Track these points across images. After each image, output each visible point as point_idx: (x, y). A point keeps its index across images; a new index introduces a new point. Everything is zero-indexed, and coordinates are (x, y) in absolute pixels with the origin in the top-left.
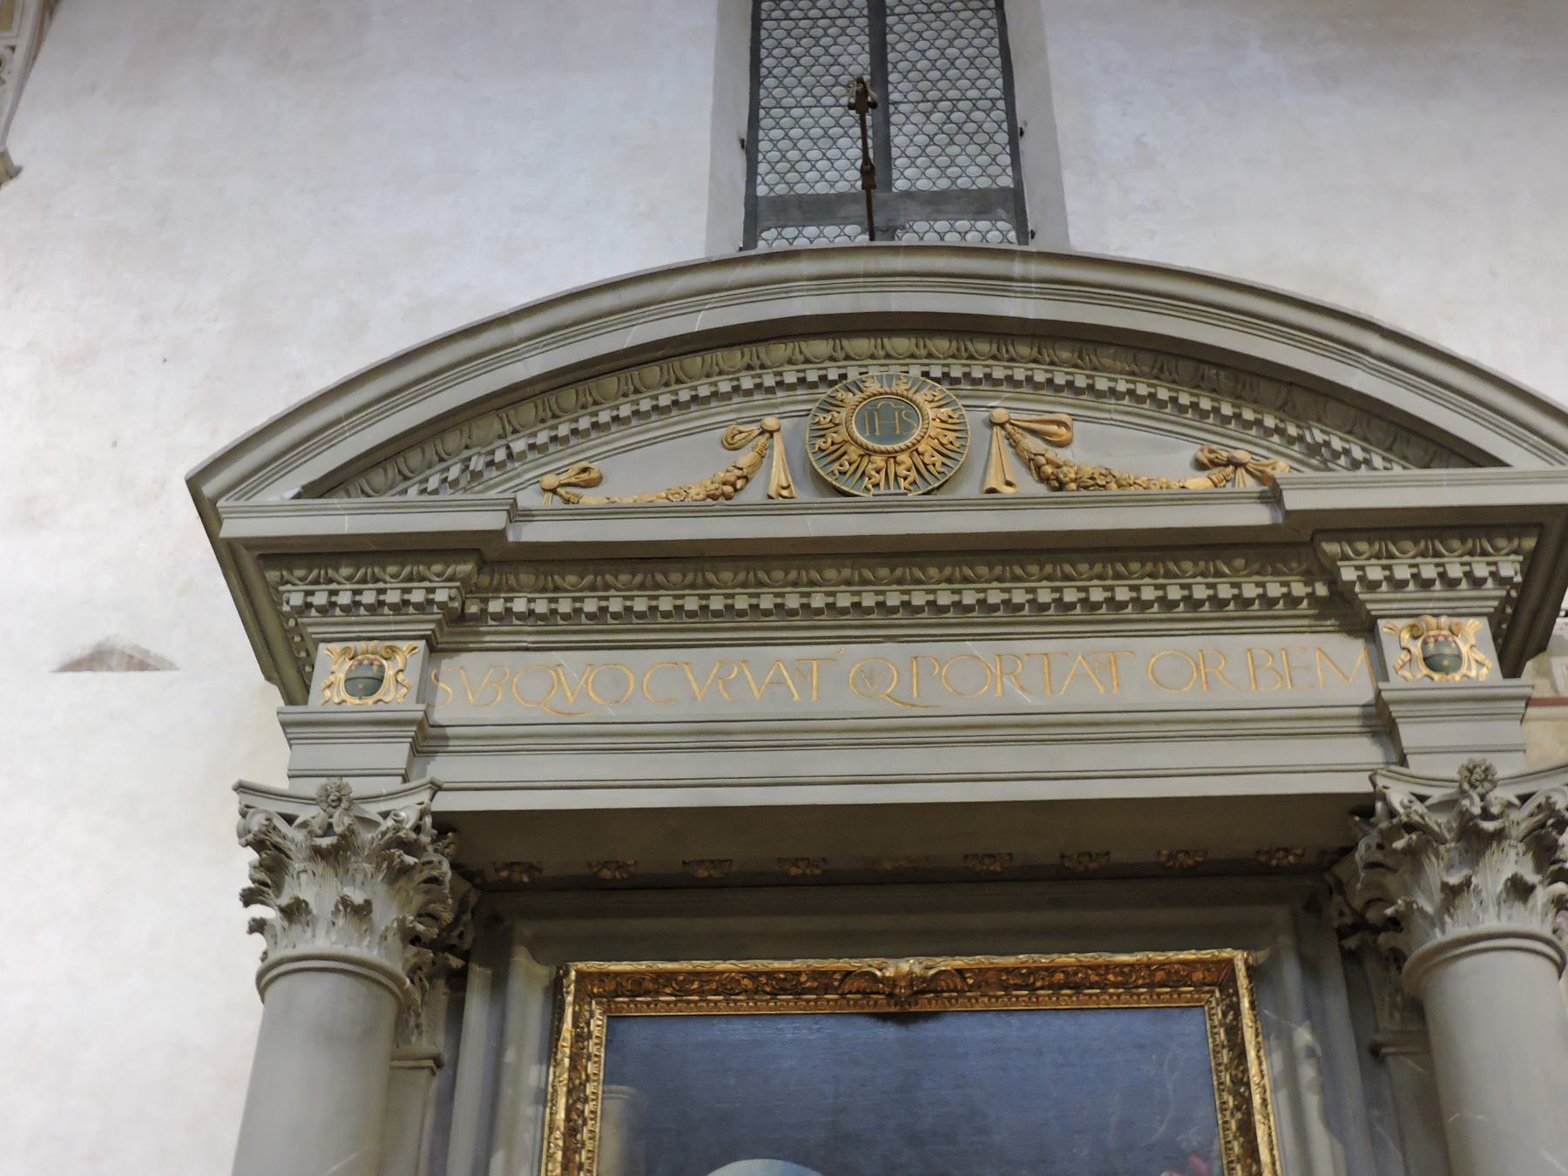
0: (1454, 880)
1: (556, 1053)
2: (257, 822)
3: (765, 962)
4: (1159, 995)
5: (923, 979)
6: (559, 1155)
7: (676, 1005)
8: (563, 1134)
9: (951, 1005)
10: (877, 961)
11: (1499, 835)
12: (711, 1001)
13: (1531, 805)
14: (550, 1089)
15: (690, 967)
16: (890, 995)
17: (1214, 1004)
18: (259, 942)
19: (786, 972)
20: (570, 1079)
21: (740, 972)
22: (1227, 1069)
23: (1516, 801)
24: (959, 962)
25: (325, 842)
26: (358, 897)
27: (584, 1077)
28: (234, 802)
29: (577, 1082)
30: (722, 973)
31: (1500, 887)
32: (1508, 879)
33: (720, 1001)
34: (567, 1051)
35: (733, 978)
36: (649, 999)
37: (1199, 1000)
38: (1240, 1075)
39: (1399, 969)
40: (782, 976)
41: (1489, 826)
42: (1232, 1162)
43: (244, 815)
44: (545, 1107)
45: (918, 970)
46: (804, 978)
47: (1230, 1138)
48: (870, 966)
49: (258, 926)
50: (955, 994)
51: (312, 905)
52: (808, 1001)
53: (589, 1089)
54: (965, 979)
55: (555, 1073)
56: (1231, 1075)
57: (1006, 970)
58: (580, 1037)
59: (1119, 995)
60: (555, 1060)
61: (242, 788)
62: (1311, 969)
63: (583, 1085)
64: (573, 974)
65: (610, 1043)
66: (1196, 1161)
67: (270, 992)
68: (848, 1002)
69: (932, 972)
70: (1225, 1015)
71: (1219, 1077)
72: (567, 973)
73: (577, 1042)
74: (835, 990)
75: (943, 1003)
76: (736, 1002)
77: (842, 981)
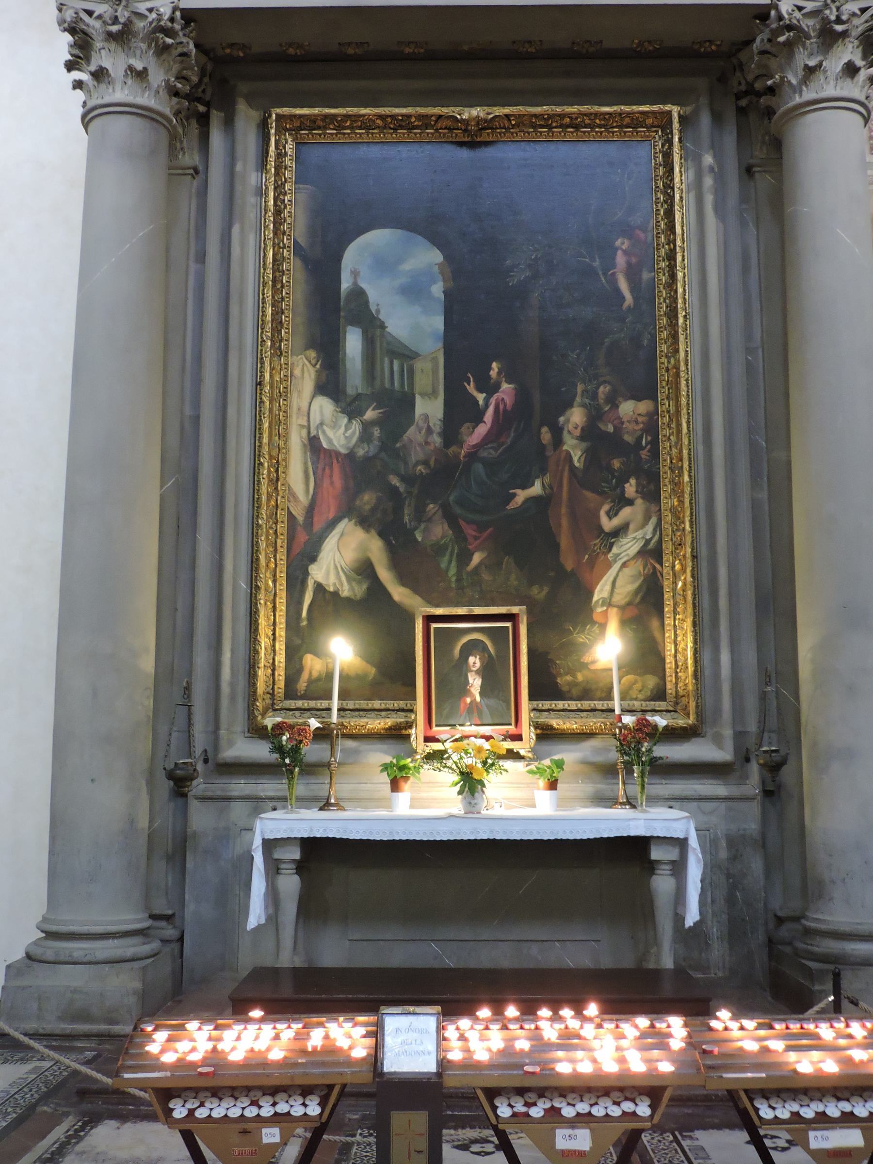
0: (812, 63)
1: (266, 165)
2: (69, 15)
3: (390, 109)
4: (625, 132)
5: (486, 121)
6: (271, 226)
7: (336, 136)
8: (273, 214)
9: (501, 137)
10: (458, 109)
11: (844, 34)
12: (357, 133)
14: (264, 187)
15: (345, 112)
16: (466, 131)
17: (657, 138)
18: (80, 95)
19: (402, 115)
20: (275, 181)
21: (375, 115)
22: (661, 179)
23: (858, 12)
24: (507, 110)
25: (115, 28)
26: (139, 66)
27: (283, 180)
29: (280, 183)
30: (364, 115)
31: (839, 68)
32: (845, 64)
33: (363, 133)
34: (273, 163)
35: (371, 119)
36: (321, 132)
37: (648, 137)
38: (669, 182)
39: (770, 119)
40: (400, 118)
41: (839, 28)
42: (659, 233)
43: (60, 10)
44: (261, 199)
45: (482, 115)
46: (413, 120)
47: (660, 219)
48: (454, 112)
49: (78, 85)
50: (504, 130)
51: (110, 71)
52: (416, 134)
53: (287, 187)
54: (510, 121)
55: (266, 177)
56: (663, 183)
57: (535, 116)
58: (280, 155)
59: (601, 133)
60: (266, 169)
62: (717, 118)
63: (283, 184)
64: (274, 116)
65: (297, 159)
66: (638, 232)
67: (90, 127)
68: (440, 135)
69: (491, 116)
70: (663, 145)
71: (656, 183)
72: (270, 116)
73: (278, 158)
74: (432, 127)
75: (496, 136)
76: (372, 134)
77: (436, 121)
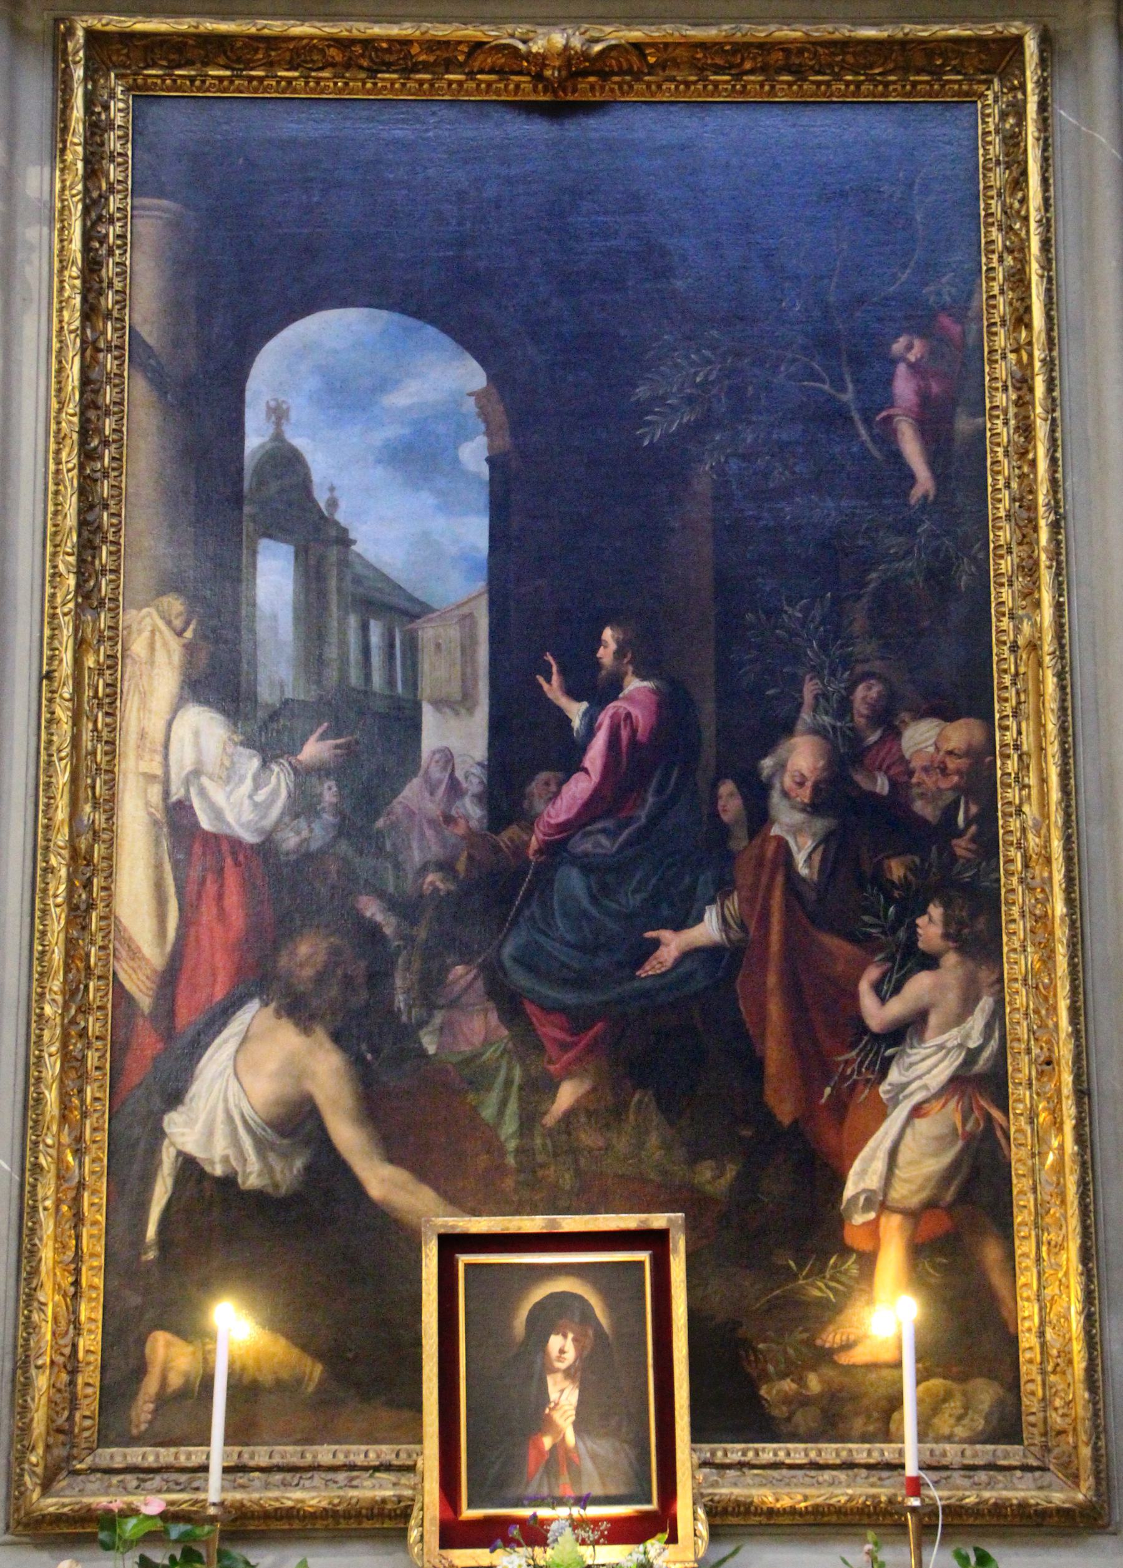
1: (63, 151)
3: (361, 26)
4: (914, 84)
5: (585, 55)
6: (77, 300)
7: (232, 82)
8: (82, 271)
9: (623, 94)
10: (520, 30)
12: (282, 78)
14: (58, 205)
15: (253, 30)
16: (539, 77)
17: (990, 101)
19: (391, 41)
20: (86, 191)
21: (327, 40)
22: (999, 195)
24: (636, 34)
27: (104, 186)
29: (95, 194)
30: (299, 38)
33: (296, 78)
34: (80, 149)
35: (314, 45)
36: (193, 73)
37: (967, 94)
38: (1016, 205)
40: (384, 45)
42: (995, 324)
44: (51, 230)
45: (577, 43)
46: (415, 50)
47: (996, 291)
48: (512, 36)
50: (628, 78)
52: (421, 83)
53: (114, 203)
54: (644, 56)
55: (63, 181)
56: (1004, 204)
57: (703, 45)
58: (95, 129)
59: (858, 85)
60: (63, 161)
63: (104, 198)
64: (80, 33)
65: (137, 132)
66: (945, 320)
68: (478, 85)
69: (598, 48)
70: (1004, 116)
71: (988, 206)
72: (70, 32)
73: (93, 134)
74: (460, 67)
75: (612, 90)
76: (318, 81)
77: (470, 55)
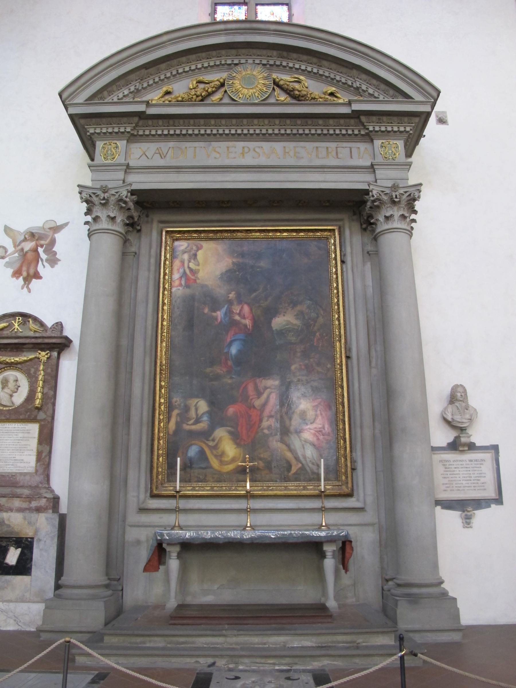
2: (84, 195)
13: (407, 194)
18: (87, 227)
25: (103, 202)
26: (112, 215)
28: (77, 189)
49: (86, 223)
51: (101, 217)
61: (79, 186)
